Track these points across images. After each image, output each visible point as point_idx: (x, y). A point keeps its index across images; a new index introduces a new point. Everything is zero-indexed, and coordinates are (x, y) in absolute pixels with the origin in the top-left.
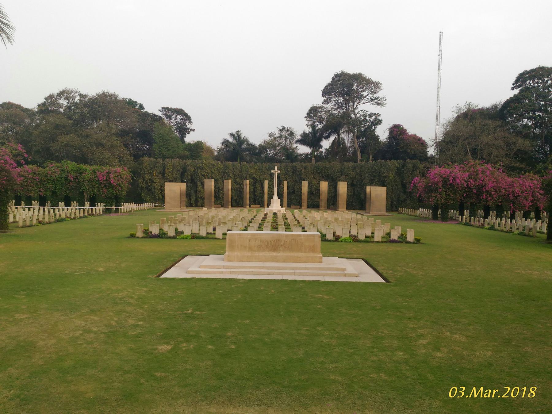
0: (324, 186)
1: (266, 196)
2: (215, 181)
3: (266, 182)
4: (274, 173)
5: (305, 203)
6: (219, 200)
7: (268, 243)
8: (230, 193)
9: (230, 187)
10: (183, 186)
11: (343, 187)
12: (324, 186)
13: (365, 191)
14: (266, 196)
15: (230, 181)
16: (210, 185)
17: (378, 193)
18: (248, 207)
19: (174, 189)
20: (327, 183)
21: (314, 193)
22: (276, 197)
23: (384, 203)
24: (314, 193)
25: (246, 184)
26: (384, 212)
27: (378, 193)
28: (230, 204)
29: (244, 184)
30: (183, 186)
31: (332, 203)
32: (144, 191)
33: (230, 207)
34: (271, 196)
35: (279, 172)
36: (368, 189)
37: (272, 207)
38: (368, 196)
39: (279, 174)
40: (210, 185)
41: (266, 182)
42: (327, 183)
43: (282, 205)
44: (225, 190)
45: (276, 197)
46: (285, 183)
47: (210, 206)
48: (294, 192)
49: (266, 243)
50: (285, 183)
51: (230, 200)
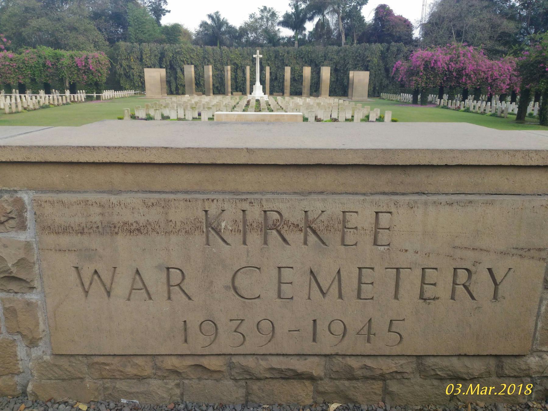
0: (307, 71)
1: (248, 83)
2: (195, 67)
3: (248, 68)
4: (255, 58)
5: (287, 90)
6: (200, 87)
8: (211, 79)
9: (211, 73)
10: (162, 72)
11: (326, 72)
12: (307, 71)
13: (348, 77)
14: (248, 83)
15: (210, 67)
16: (190, 71)
17: (360, 78)
18: (230, 94)
19: (154, 76)
20: (310, 68)
21: (297, 79)
22: (258, 83)
23: (367, 88)
24: (297, 79)
25: (227, 71)
26: (366, 97)
27: (360, 78)
28: (212, 91)
29: (226, 71)
30: (162, 72)
31: (315, 90)
32: (124, 78)
33: (212, 94)
34: (253, 83)
35: (261, 56)
36: (351, 74)
37: (255, 94)
38: (350, 82)
40: (190, 71)
41: (248, 68)
42: (310, 68)
43: (264, 91)
44: (205, 76)
45: (258, 83)
46: (268, 69)
47: (191, 93)
48: (276, 79)
50: (268, 69)
51: (211, 87)
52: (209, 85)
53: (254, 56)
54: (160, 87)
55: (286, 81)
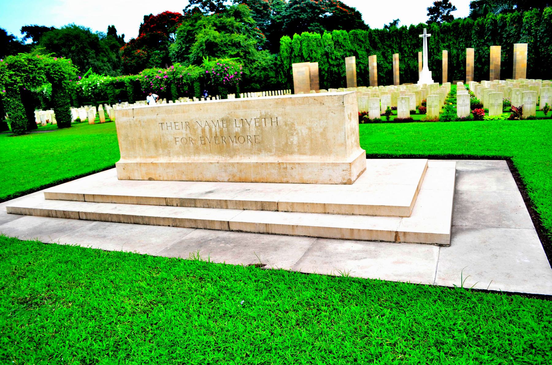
0: (496, 52)
4: (422, 39)
6: (363, 79)
7: (203, 131)
8: (376, 71)
9: (375, 64)
15: (375, 57)
16: (351, 63)
20: (499, 48)
21: (482, 62)
24: (482, 62)
25: (395, 59)
30: (314, 67)
39: (428, 38)
40: (351, 63)
42: (499, 48)
43: (437, 78)
44: (370, 68)
49: (199, 131)
51: (376, 79)
52: (374, 77)
53: (420, 36)
54: (309, 82)
55: (469, 65)
